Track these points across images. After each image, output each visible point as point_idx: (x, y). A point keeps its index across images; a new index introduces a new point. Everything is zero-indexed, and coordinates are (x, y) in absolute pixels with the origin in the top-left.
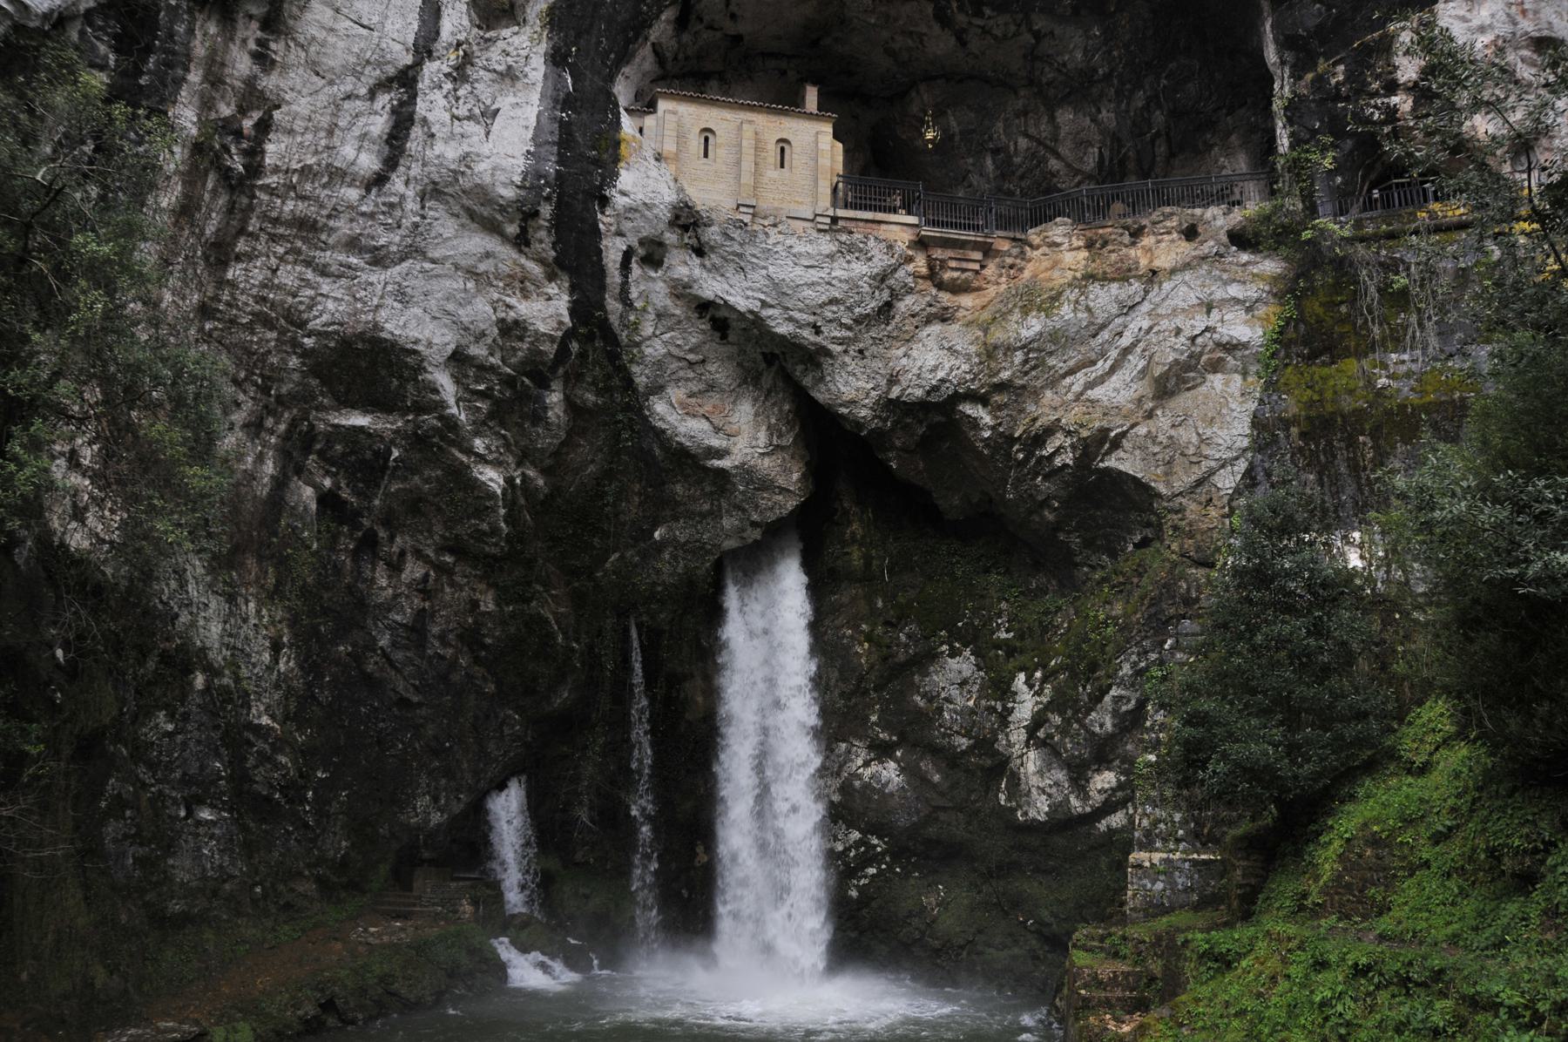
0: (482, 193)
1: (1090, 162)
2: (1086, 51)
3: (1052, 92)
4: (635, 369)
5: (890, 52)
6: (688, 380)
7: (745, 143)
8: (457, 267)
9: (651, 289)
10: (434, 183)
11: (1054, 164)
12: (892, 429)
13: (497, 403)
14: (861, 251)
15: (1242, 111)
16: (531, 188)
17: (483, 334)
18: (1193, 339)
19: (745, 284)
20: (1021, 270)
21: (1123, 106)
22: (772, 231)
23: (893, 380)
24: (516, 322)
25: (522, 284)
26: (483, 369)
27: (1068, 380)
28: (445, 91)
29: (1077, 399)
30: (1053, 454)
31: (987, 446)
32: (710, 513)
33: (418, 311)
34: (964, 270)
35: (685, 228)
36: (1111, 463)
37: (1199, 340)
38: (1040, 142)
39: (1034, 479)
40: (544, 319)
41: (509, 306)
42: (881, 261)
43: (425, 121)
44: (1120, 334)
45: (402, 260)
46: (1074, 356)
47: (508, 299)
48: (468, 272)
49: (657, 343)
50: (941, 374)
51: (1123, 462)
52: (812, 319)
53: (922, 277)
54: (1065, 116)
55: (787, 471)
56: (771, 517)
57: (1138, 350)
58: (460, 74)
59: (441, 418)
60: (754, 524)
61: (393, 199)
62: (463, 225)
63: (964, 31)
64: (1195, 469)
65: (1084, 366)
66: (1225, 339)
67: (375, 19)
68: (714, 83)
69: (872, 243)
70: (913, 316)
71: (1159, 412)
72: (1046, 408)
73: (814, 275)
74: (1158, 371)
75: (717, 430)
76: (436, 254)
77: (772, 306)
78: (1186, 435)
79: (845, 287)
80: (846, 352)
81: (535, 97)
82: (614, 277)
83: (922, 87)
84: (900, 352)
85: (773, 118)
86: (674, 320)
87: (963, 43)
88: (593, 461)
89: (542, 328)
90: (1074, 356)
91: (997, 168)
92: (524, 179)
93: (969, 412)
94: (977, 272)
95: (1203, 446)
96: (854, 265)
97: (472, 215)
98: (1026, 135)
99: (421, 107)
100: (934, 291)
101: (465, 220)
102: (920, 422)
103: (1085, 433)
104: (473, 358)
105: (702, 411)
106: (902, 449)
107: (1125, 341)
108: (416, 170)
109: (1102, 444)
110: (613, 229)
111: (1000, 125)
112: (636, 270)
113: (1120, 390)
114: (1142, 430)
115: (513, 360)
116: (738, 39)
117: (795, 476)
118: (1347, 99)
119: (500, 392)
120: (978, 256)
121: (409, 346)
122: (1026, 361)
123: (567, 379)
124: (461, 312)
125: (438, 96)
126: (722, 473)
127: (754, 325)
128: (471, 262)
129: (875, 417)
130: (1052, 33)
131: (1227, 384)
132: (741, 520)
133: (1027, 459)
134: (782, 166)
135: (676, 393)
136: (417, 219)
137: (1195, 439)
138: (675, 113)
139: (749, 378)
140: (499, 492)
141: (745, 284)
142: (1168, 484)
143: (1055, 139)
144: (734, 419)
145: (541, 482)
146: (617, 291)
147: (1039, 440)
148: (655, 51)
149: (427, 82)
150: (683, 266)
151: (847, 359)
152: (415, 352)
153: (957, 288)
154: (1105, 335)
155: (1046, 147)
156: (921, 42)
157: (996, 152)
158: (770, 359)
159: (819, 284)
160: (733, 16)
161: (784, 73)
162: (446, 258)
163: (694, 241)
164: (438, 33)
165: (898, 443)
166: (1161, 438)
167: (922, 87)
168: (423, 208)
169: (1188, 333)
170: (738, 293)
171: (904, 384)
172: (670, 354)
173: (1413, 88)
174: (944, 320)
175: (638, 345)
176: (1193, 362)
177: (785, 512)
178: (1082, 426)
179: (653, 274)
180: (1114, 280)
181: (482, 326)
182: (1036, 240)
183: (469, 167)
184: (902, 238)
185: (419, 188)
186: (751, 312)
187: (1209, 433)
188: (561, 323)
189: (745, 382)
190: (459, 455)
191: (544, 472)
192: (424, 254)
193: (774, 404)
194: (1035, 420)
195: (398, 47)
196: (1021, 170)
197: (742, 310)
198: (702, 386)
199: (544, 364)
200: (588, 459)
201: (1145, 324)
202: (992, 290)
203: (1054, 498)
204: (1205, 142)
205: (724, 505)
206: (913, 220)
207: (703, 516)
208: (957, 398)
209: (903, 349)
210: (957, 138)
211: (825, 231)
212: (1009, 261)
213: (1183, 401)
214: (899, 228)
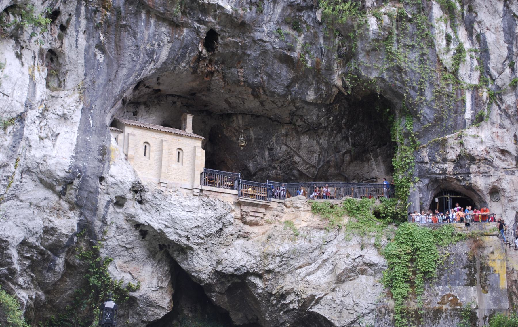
0: (50, 174)
1: (314, 160)
2: (318, 116)
3: (300, 129)
4: (101, 250)
5: (227, 102)
6: (125, 255)
7: (164, 151)
8: (31, 204)
9: (116, 217)
10: (28, 167)
11: (297, 159)
12: (215, 284)
13: (33, 261)
14: (212, 205)
15: (384, 147)
16: (73, 173)
17: (37, 233)
18: (354, 259)
19: (159, 217)
20: (281, 217)
21: (332, 139)
22: (173, 194)
23: (219, 262)
24: (52, 228)
25: (57, 211)
26: (31, 247)
27: (299, 271)
28: (36, 125)
29: (302, 280)
30: (289, 303)
31: (260, 296)
32: (123, 315)
33: (11, 223)
34: (256, 217)
35: (136, 192)
36: (315, 310)
37: (357, 260)
38: (292, 149)
39: (279, 312)
40: (65, 227)
41: (50, 221)
42: (221, 211)
43: (27, 139)
44: (323, 253)
45: (8, 200)
47: (50, 218)
48: (35, 206)
49: (114, 240)
50: (242, 263)
52: (186, 234)
53: (238, 219)
54: (305, 139)
55: (163, 298)
56: (152, 319)
57: (330, 261)
58: (42, 116)
59: (9, 269)
60: (143, 322)
61: (10, 174)
62: (36, 185)
63: (264, 101)
64: (351, 316)
65: (306, 265)
66: (368, 262)
67: (10, 91)
68: (142, 107)
69: (217, 202)
70: (231, 235)
71: (337, 289)
73: (190, 215)
74: (338, 272)
75: (134, 278)
76: (22, 198)
77: (170, 227)
78: (348, 301)
79: (203, 221)
80: (199, 248)
81: (76, 129)
82: (101, 211)
83: (240, 117)
84: (224, 251)
85: (175, 137)
86: (124, 230)
87: (262, 103)
88: (70, 289)
89: (64, 231)
91: (270, 156)
92: (70, 169)
93: (253, 281)
94: (262, 218)
95: (355, 306)
96: (208, 212)
97: (41, 181)
98: (286, 145)
99: (26, 133)
100: (242, 225)
101: (38, 183)
102: (229, 281)
103: (304, 296)
104: (29, 243)
105: (129, 270)
106: (219, 293)
107: (325, 257)
109: (311, 301)
110: (105, 191)
111: (274, 139)
112: (111, 208)
114: (329, 297)
115: (46, 244)
116: (159, 90)
117: (167, 301)
118: (427, 163)
119: (36, 257)
120: (263, 210)
121: (5, 239)
122: (281, 262)
123: (68, 253)
124: (30, 223)
125: (33, 127)
126: (133, 299)
127: (160, 235)
128: (38, 202)
129: (210, 278)
130: (304, 108)
131: (367, 280)
132: (138, 320)
133: (277, 304)
134: (178, 162)
135: (118, 262)
136: (18, 183)
137: (352, 303)
138: (134, 135)
139: (152, 254)
140: (25, 303)
141: (159, 217)
142: (339, 321)
143: (299, 148)
144: (142, 274)
145: (43, 297)
146: (101, 217)
147: (283, 296)
148: (123, 100)
149: (29, 121)
150: (132, 207)
151: (199, 252)
152: (6, 241)
153: (251, 224)
154: (316, 252)
155: (295, 152)
156: (243, 101)
157: (271, 149)
158: (162, 247)
159: (192, 219)
160: (159, 84)
161: (175, 103)
162: (27, 200)
163: (139, 198)
164: (35, 96)
165: (217, 290)
166: (338, 301)
167: (240, 117)
168: (21, 178)
169: (353, 257)
170: (154, 221)
171: (224, 265)
172: (119, 244)
174: (245, 238)
175: (105, 240)
176: (354, 268)
177: (159, 317)
178: (303, 293)
179: (118, 210)
180: (322, 229)
181: (37, 230)
182: (288, 204)
183: (45, 161)
185: (21, 169)
186: (160, 230)
187: (358, 301)
188: (73, 229)
189: (149, 257)
190: (11, 285)
191: (47, 292)
192: (18, 198)
193: (161, 267)
194: (282, 288)
195: (18, 105)
196: (281, 159)
197: (156, 228)
198: (130, 259)
199: (60, 246)
200: (70, 288)
201: (335, 250)
202: (267, 227)
203: (287, 322)
204: (367, 158)
205: (131, 312)
206: (235, 192)
208: (248, 274)
209: (225, 249)
210: (253, 141)
211: (197, 195)
212: (276, 213)
213: (347, 286)
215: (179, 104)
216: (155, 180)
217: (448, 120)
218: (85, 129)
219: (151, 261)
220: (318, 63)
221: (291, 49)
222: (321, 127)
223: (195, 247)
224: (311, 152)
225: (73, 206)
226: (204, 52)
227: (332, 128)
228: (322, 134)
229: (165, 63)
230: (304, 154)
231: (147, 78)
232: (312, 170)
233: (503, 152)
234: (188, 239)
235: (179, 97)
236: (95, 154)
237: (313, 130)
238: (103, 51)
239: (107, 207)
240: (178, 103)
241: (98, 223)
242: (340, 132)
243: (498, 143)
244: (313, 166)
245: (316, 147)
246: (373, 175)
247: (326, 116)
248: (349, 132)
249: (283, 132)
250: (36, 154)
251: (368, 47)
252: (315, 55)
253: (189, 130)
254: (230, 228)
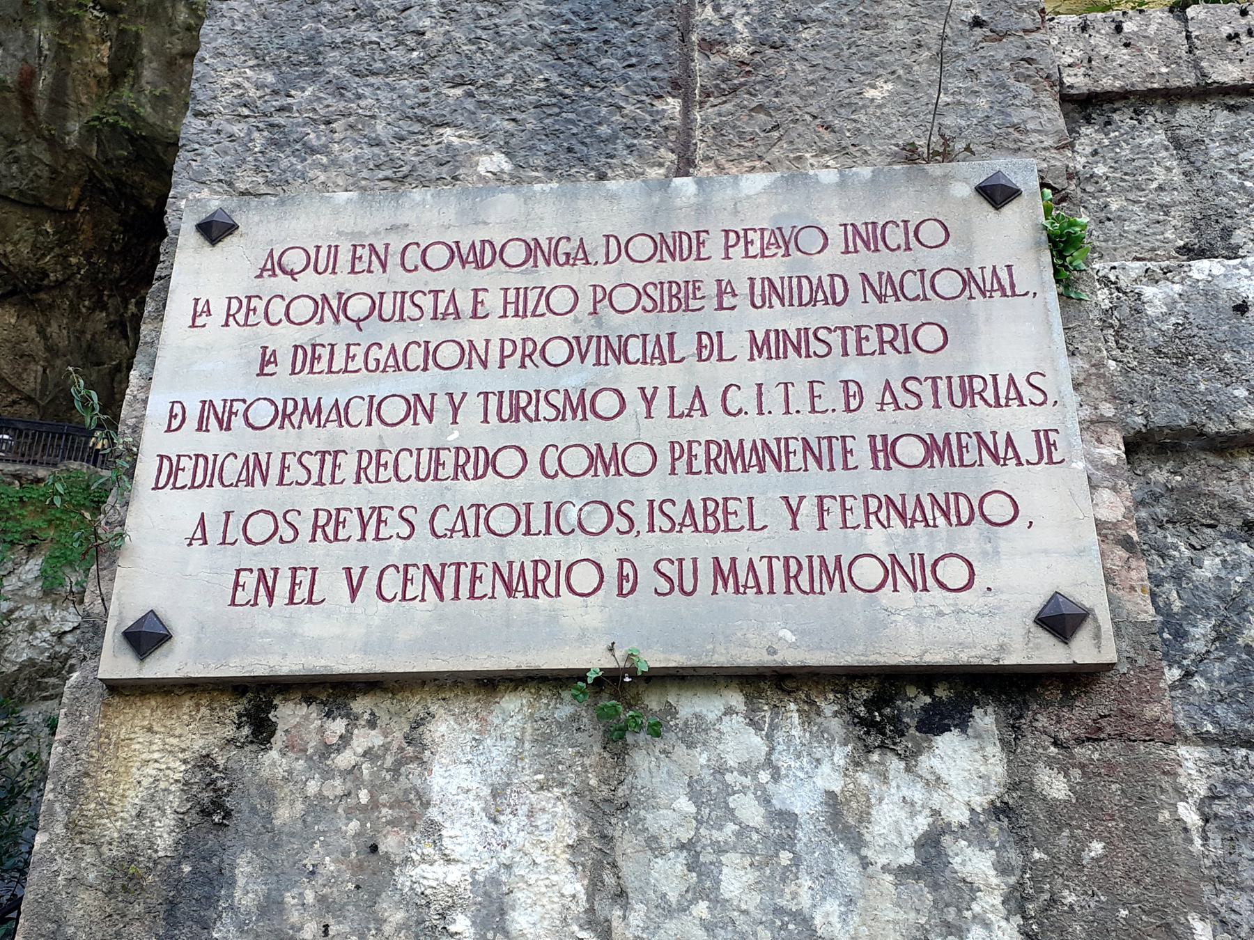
18: (60, 635)
37: (69, 638)
169: (55, 627)
222: (45, 282)
227: (78, 289)
228: (51, 307)
232: (27, 410)
244: (29, 399)
245: (36, 345)
247: (57, 250)
248: (126, 307)
252: (20, 54)
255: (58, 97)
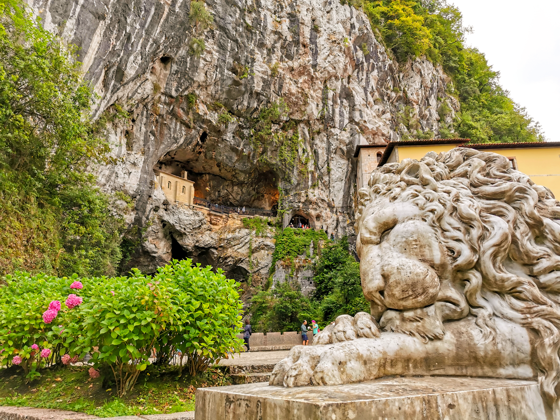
1: (238, 198)
5: (203, 167)
11: (231, 197)
36: (240, 265)
43: (116, 173)
46: (237, 242)
51: (243, 265)
54: (236, 188)
72: (229, 252)
73: (187, 218)
74: (253, 248)
75: (156, 247)
81: (140, 171)
87: (220, 170)
90: (237, 242)
107: (246, 241)
108: (112, 184)
112: (152, 212)
113: (244, 251)
114: (247, 259)
120: (219, 218)
126: (154, 257)
135: (150, 239)
139: (165, 236)
143: (232, 192)
147: (226, 258)
150: (162, 212)
153: (214, 224)
154: (243, 239)
157: (219, 191)
158: (170, 233)
161: (178, 165)
170: (170, 219)
173: (303, 203)
182: (230, 216)
184: (206, 212)
195: (114, 155)
206: (208, 209)
207: (145, 266)
208: (211, 247)
213: (255, 255)
214: (205, 210)
215: (180, 166)
216: (173, 200)
217: (302, 185)
218: (144, 171)
219: (164, 239)
220: (249, 154)
221: (239, 146)
223: (188, 234)
224: (238, 194)
225: (135, 209)
226: (200, 142)
229: (181, 145)
230: (234, 195)
231: (172, 151)
232: (236, 202)
233: (323, 200)
234: (185, 229)
235: (180, 162)
236: (148, 184)
237: (241, 184)
238: (154, 135)
239: (150, 211)
240: (180, 166)
241: (144, 219)
242: (252, 186)
243: (321, 196)
244: (237, 201)
245: (240, 192)
246: (263, 206)
249: (227, 184)
250: (120, 181)
251: (273, 149)
253: (186, 178)
254: (204, 225)
255: (253, 157)
